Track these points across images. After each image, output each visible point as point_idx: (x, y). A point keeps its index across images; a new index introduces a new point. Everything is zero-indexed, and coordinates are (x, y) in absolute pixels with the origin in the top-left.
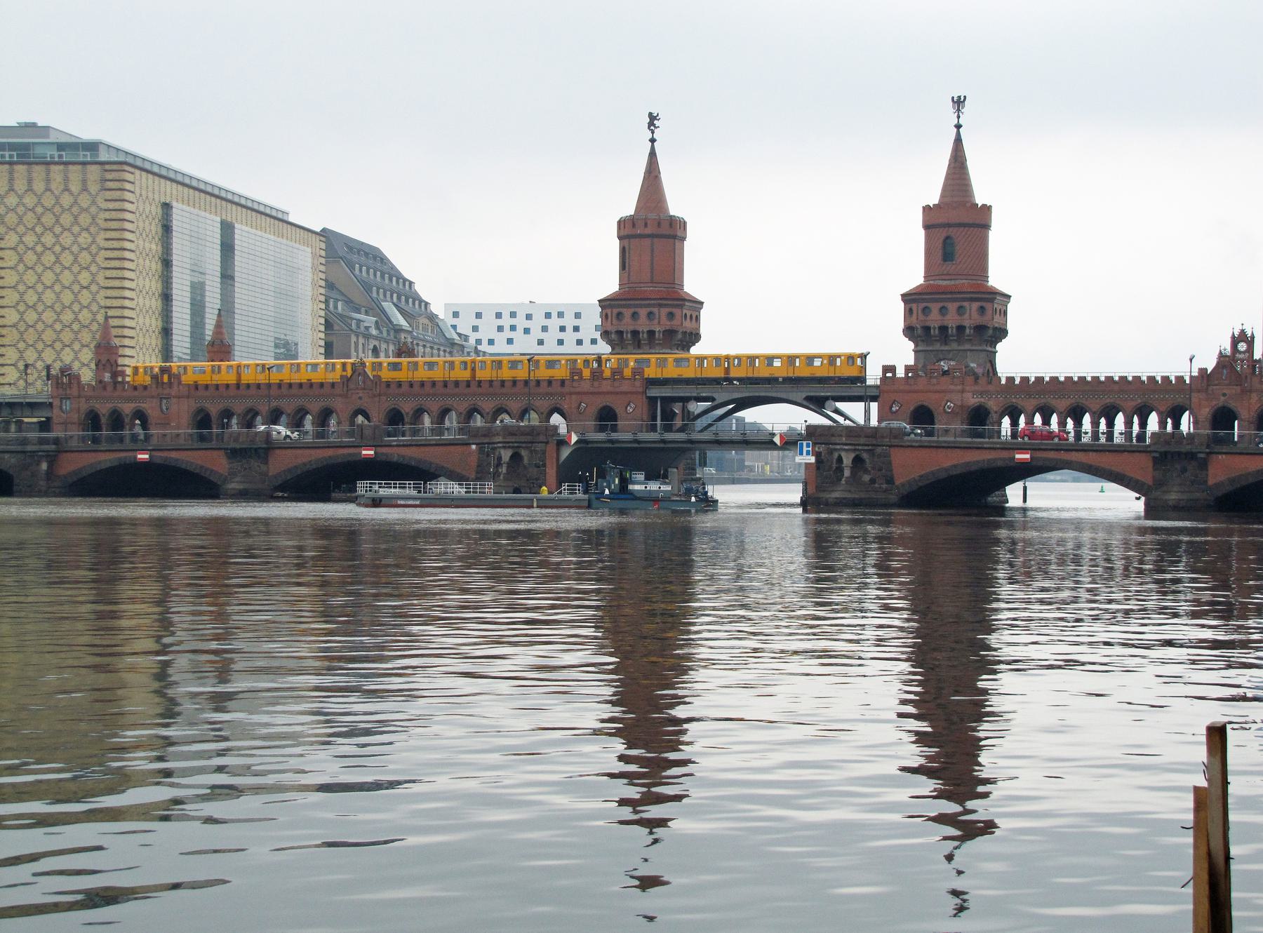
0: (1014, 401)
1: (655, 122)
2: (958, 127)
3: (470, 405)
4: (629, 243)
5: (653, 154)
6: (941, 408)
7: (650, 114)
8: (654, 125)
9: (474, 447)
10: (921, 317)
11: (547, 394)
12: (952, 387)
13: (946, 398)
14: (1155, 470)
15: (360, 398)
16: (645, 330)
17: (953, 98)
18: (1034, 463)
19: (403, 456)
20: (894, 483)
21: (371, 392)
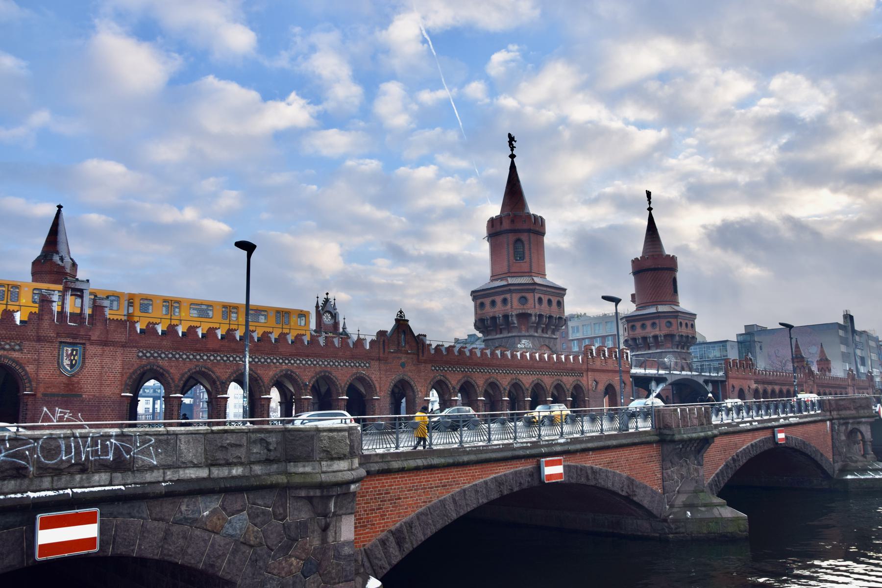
5: (513, 167)
7: (510, 135)
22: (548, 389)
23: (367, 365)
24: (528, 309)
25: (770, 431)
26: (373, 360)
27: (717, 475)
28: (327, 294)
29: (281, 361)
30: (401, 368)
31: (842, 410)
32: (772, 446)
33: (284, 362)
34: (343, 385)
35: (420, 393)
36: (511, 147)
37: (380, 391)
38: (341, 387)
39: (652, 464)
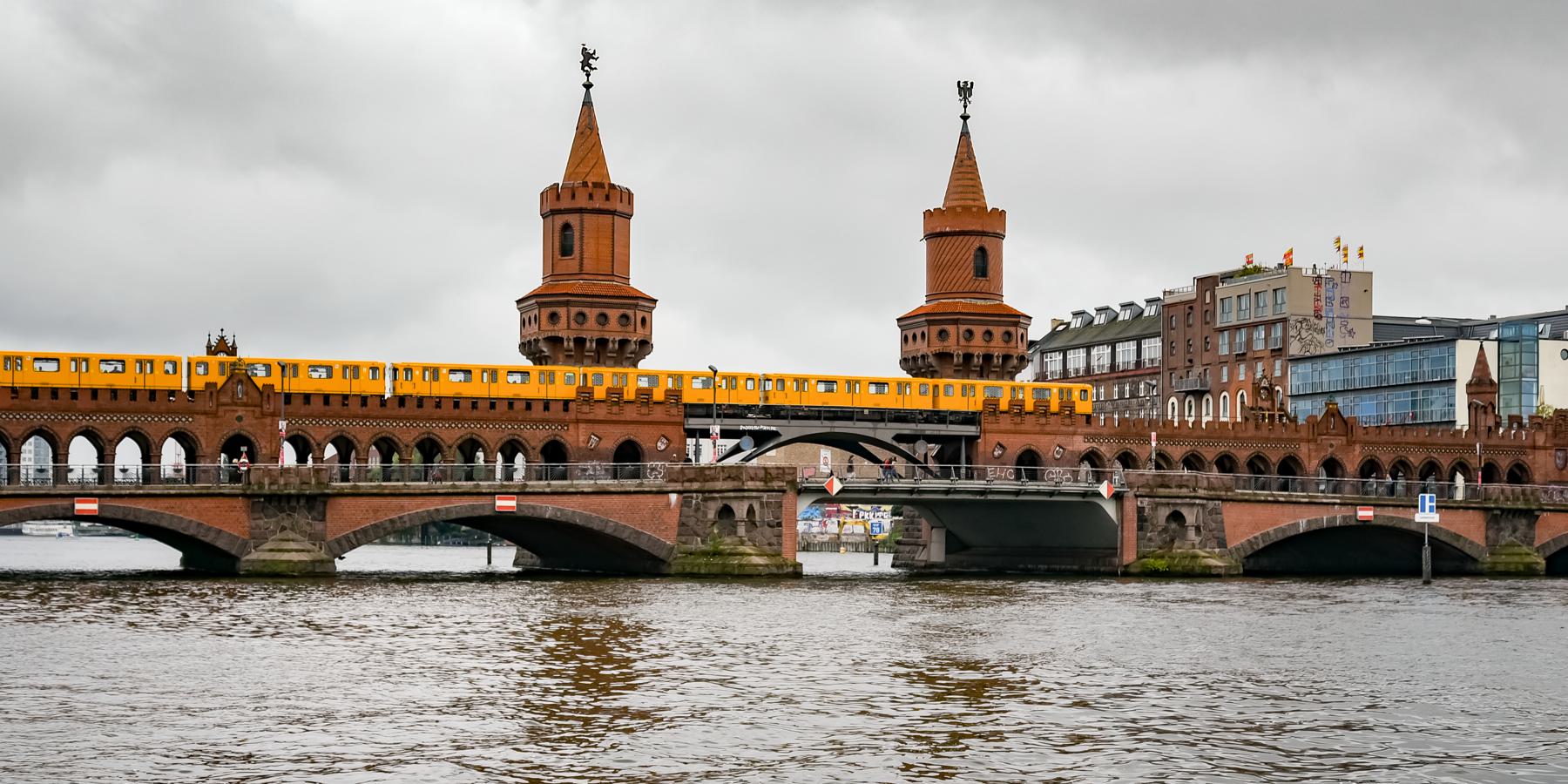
0: (1128, 446)
1: (591, 61)
2: (965, 118)
3: (420, 435)
4: (582, 221)
5: (587, 104)
6: (1050, 454)
8: (589, 66)
9: (673, 497)
10: (962, 342)
11: (543, 421)
12: (1063, 428)
13: (1057, 442)
14: (1487, 529)
15: (240, 419)
16: (617, 339)
17: (959, 82)
18: (1379, 522)
19: (559, 509)
20: (1226, 548)
21: (258, 410)
22: (492, 446)
23: (190, 419)
24: (559, 331)
25: (489, 498)
26: (197, 414)
27: (354, 532)
28: (222, 330)
29: (81, 418)
30: (237, 422)
31: (708, 481)
32: (487, 512)
33: (84, 418)
34: (157, 442)
35: (264, 451)
36: (584, 71)
37: (207, 446)
38: (155, 443)
39: (234, 513)
